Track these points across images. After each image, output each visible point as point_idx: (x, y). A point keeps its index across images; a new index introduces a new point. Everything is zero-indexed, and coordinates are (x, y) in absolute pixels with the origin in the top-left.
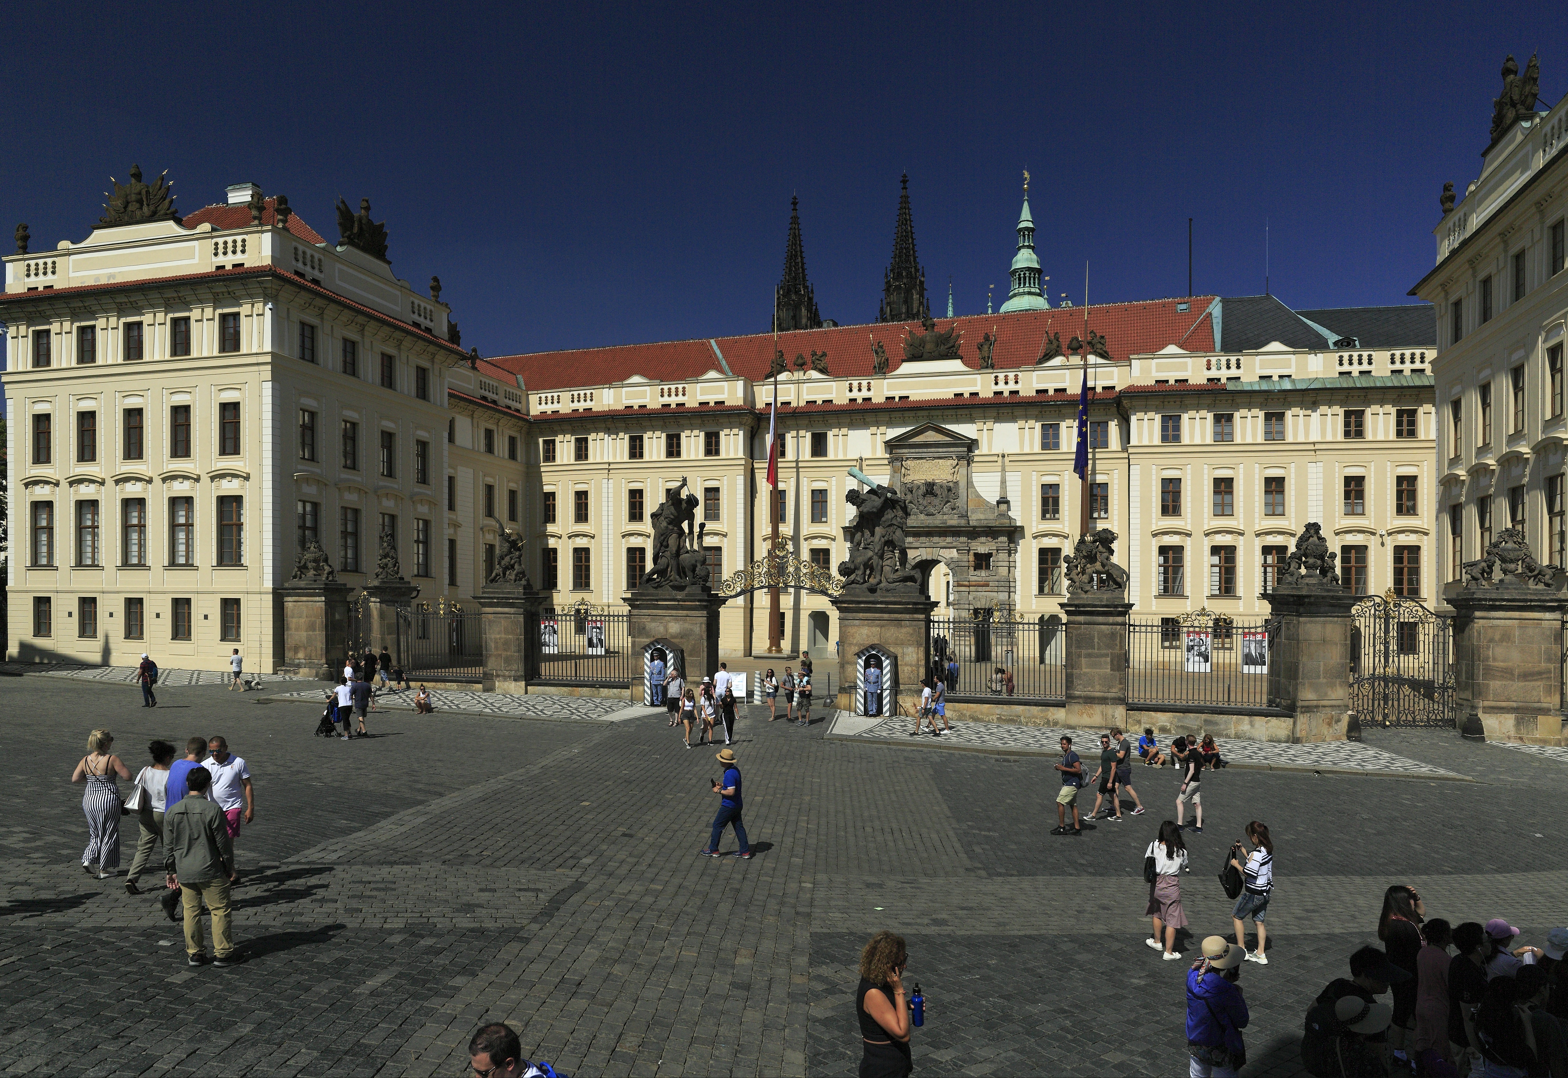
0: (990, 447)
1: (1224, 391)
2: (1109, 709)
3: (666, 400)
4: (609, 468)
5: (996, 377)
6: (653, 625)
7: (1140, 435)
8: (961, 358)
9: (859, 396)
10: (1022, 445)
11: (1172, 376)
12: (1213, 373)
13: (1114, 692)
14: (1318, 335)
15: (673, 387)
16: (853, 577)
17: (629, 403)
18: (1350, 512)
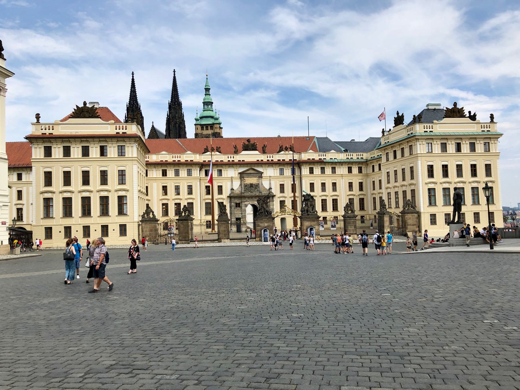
0: (266, 174)
1: (323, 162)
2: (354, 235)
3: (174, 159)
4: (155, 179)
5: (267, 156)
6: (261, 224)
7: (304, 172)
8: (258, 150)
9: (231, 160)
10: (274, 174)
11: (311, 158)
12: (320, 157)
13: (355, 232)
14: (340, 148)
15: (176, 155)
16: (304, 212)
17: (162, 159)
18: (350, 190)
